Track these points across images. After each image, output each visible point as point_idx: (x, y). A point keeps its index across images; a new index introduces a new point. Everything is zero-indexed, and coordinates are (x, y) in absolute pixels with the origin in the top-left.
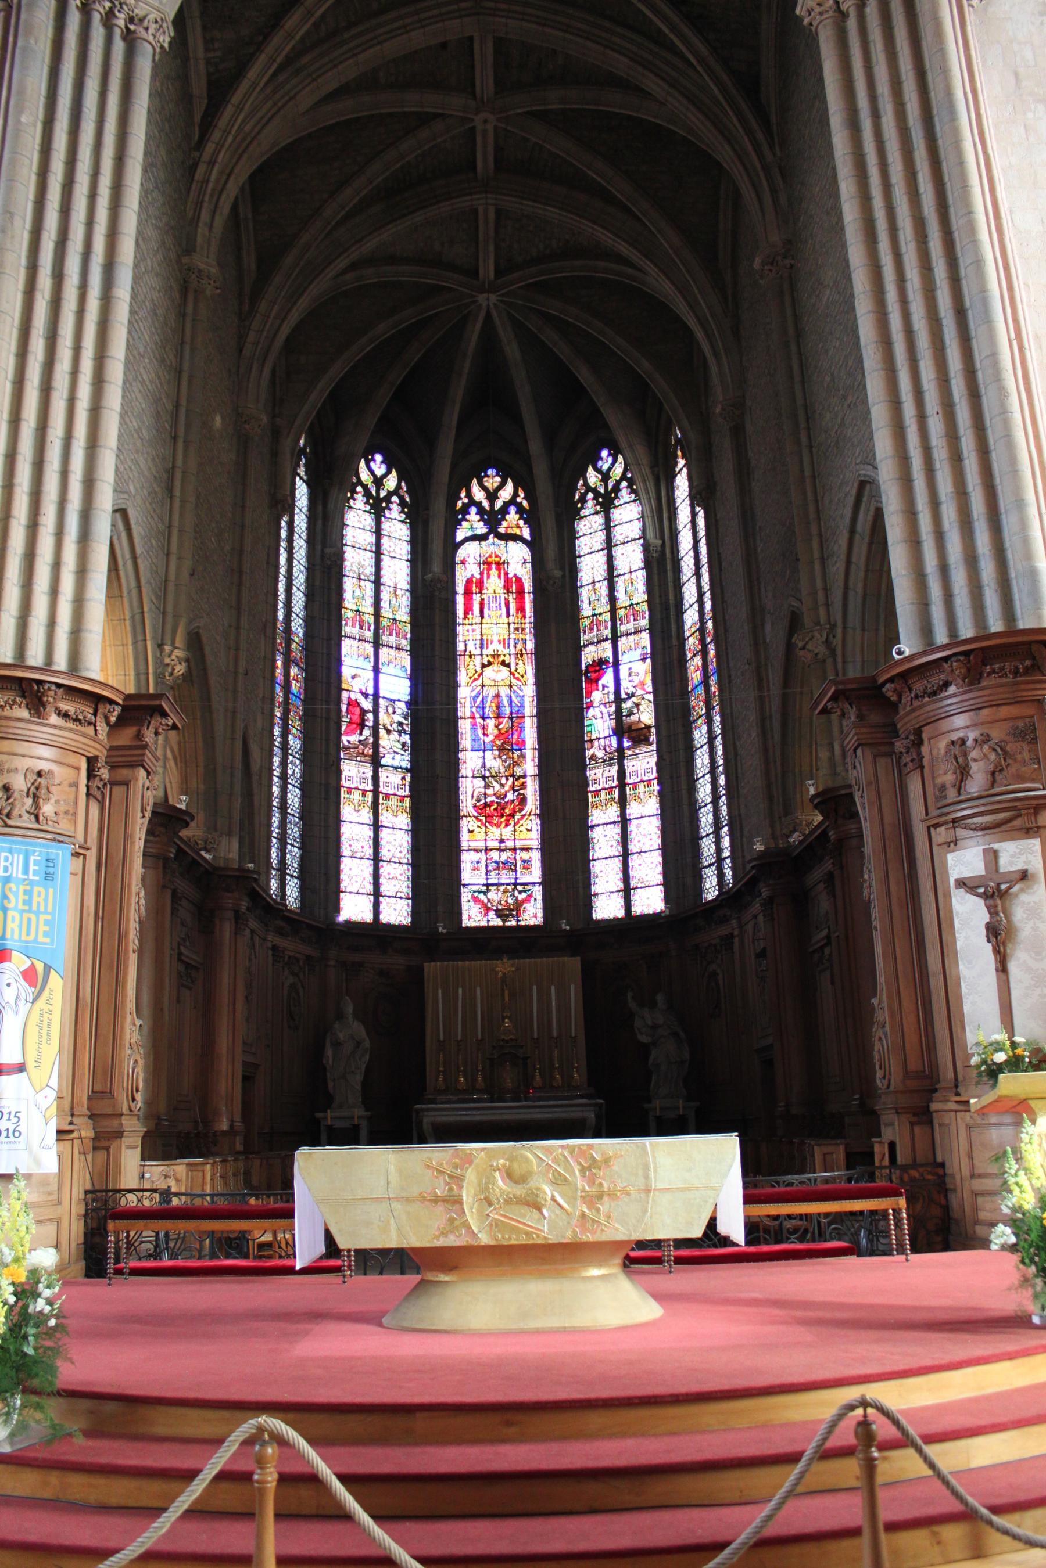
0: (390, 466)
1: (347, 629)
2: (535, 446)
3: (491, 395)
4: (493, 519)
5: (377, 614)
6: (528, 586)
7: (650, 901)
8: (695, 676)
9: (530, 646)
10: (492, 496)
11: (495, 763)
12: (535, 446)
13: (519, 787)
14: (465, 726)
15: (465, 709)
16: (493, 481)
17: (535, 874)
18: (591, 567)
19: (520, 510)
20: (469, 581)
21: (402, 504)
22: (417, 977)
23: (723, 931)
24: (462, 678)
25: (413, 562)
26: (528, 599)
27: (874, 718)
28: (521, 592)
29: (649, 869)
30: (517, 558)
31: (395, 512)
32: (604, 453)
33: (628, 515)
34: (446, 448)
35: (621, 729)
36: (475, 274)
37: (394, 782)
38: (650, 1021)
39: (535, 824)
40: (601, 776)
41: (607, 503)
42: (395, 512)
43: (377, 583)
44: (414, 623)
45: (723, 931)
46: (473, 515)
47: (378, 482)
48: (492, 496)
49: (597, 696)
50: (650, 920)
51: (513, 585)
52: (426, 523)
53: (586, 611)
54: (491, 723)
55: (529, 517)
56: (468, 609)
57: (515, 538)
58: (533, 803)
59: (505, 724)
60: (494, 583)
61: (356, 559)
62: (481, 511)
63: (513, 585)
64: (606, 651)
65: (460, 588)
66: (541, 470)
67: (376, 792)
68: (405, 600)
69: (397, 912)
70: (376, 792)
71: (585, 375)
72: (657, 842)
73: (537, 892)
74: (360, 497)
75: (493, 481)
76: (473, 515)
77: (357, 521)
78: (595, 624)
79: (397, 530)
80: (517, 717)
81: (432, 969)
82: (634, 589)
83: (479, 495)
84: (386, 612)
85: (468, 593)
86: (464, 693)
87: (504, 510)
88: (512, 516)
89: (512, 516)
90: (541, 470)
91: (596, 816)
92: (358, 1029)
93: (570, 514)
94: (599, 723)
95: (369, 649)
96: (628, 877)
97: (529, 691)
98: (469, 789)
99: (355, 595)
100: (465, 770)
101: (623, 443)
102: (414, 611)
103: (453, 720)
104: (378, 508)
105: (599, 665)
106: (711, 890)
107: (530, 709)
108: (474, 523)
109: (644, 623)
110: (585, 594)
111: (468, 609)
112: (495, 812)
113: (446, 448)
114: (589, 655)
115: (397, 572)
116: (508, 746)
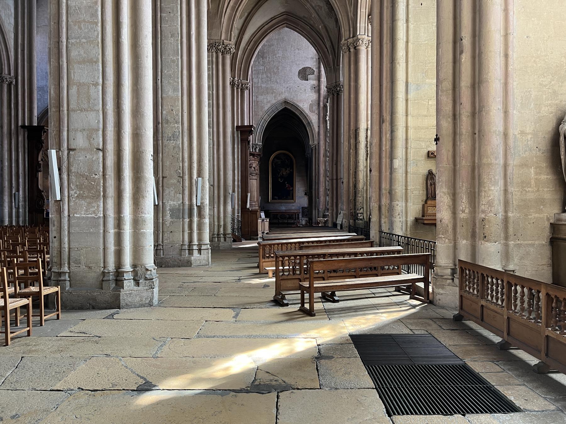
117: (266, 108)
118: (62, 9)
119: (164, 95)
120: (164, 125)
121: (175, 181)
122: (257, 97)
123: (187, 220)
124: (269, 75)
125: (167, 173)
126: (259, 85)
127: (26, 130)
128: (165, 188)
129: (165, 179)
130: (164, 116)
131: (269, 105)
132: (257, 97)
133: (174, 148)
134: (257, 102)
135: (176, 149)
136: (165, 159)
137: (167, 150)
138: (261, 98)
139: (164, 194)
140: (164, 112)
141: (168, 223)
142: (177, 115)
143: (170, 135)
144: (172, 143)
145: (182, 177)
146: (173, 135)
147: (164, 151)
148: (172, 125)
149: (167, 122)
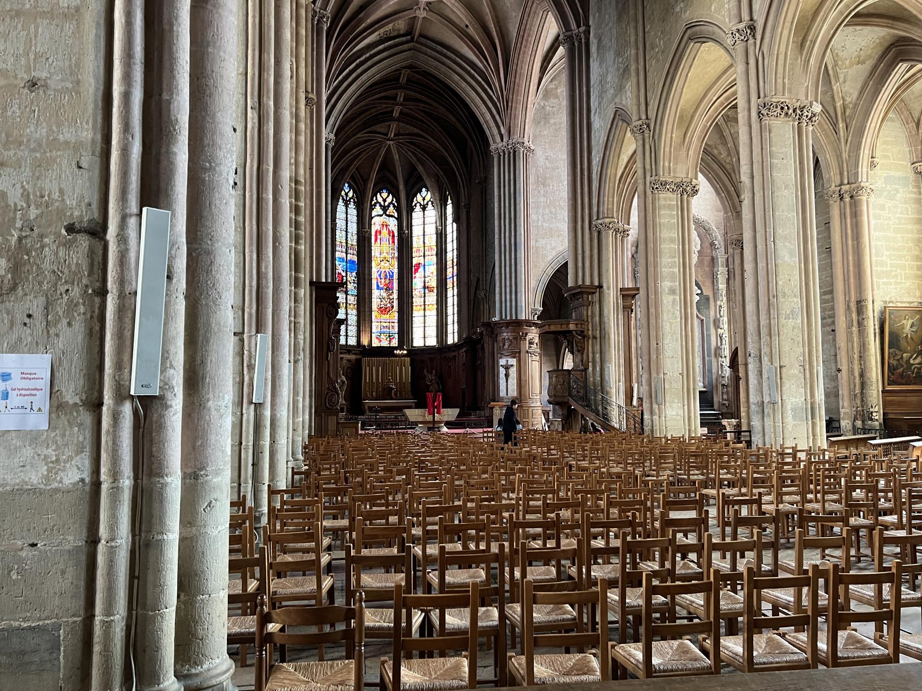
0: (350, 187)
1: (337, 248)
2: (401, 187)
3: (387, 167)
4: (385, 209)
5: (347, 243)
6: (396, 234)
7: (432, 342)
8: (449, 274)
9: (396, 255)
10: (385, 201)
11: (385, 295)
12: (401, 187)
14: (374, 282)
15: (375, 275)
16: (385, 195)
17: (396, 330)
18: (417, 231)
19: (394, 206)
20: (376, 232)
21: (354, 202)
22: (358, 362)
23: (453, 354)
24: (373, 264)
25: (358, 223)
26: (396, 238)
27: (489, 329)
28: (393, 236)
29: (432, 332)
30: (393, 224)
31: (352, 205)
32: (424, 189)
33: (432, 214)
34: (371, 185)
35: (425, 287)
36: (387, 135)
37: (352, 300)
38: (430, 377)
39: (396, 315)
40: (417, 301)
41: (424, 208)
42: (352, 205)
43: (347, 231)
44: (358, 245)
45: (453, 354)
46: (378, 207)
47: (347, 194)
48: (385, 201)
49: (417, 275)
50: (431, 348)
51: (391, 233)
52: (362, 210)
53: (415, 245)
54: (383, 281)
55: (398, 209)
56: (376, 240)
57: (392, 216)
58: (396, 308)
59: (387, 281)
61: (340, 223)
62: (381, 205)
63: (391, 233)
64: (421, 260)
65: (373, 233)
67: (346, 303)
68: (355, 237)
69: (352, 341)
70: (346, 303)
71: (420, 168)
72: (435, 324)
73: (396, 336)
74: (341, 200)
75: (385, 195)
76: (378, 207)
77: (341, 207)
78: (418, 250)
79: (353, 211)
81: (365, 360)
82: (432, 241)
83: (380, 200)
84: (349, 242)
85: (376, 236)
86: (374, 270)
87: (389, 206)
88: (391, 207)
89: (391, 207)
91: (415, 313)
92: (344, 378)
93: (411, 209)
94: (417, 283)
95: (344, 255)
96: (424, 334)
97: (396, 271)
99: (340, 236)
100: (374, 296)
101: (428, 185)
102: (358, 241)
104: (347, 206)
105: (418, 265)
106: (450, 341)
107: (396, 276)
108: (378, 210)
109: (435, 253)
110: (414, 239)
111: (376, 240)
112: (383, 310)
113: (371, 185)
115: (353, 228)
116: (388, 288)
117: (550, 258)
118: (172, 88)
119: (779, 262)
120: (781, 299)
121: (796, 372)
122: (536, 241)
123: (810, 423)
124: (553, 210)
125: (785, 361)
126: (540, 224)
127: (314, 288)
128: (784, 380)
129: (784, 370)
130: (779, 288)
131: (554, 253)
132: (536, 241)
133: (794, 328)
134: (537, 248)
135: (796, 330)
136: (783, 343)
137: (785, 331)
138: (542, 242)
139: (784, 389)
140: (780, 283)
141: (789, 427)
142: (796, 286)
143: (788, 312)
144: (791, 322)
145: (803, 366)
146: (792, 312)
147: (781, 333)
148: (790, 299)
149: (784, 295)
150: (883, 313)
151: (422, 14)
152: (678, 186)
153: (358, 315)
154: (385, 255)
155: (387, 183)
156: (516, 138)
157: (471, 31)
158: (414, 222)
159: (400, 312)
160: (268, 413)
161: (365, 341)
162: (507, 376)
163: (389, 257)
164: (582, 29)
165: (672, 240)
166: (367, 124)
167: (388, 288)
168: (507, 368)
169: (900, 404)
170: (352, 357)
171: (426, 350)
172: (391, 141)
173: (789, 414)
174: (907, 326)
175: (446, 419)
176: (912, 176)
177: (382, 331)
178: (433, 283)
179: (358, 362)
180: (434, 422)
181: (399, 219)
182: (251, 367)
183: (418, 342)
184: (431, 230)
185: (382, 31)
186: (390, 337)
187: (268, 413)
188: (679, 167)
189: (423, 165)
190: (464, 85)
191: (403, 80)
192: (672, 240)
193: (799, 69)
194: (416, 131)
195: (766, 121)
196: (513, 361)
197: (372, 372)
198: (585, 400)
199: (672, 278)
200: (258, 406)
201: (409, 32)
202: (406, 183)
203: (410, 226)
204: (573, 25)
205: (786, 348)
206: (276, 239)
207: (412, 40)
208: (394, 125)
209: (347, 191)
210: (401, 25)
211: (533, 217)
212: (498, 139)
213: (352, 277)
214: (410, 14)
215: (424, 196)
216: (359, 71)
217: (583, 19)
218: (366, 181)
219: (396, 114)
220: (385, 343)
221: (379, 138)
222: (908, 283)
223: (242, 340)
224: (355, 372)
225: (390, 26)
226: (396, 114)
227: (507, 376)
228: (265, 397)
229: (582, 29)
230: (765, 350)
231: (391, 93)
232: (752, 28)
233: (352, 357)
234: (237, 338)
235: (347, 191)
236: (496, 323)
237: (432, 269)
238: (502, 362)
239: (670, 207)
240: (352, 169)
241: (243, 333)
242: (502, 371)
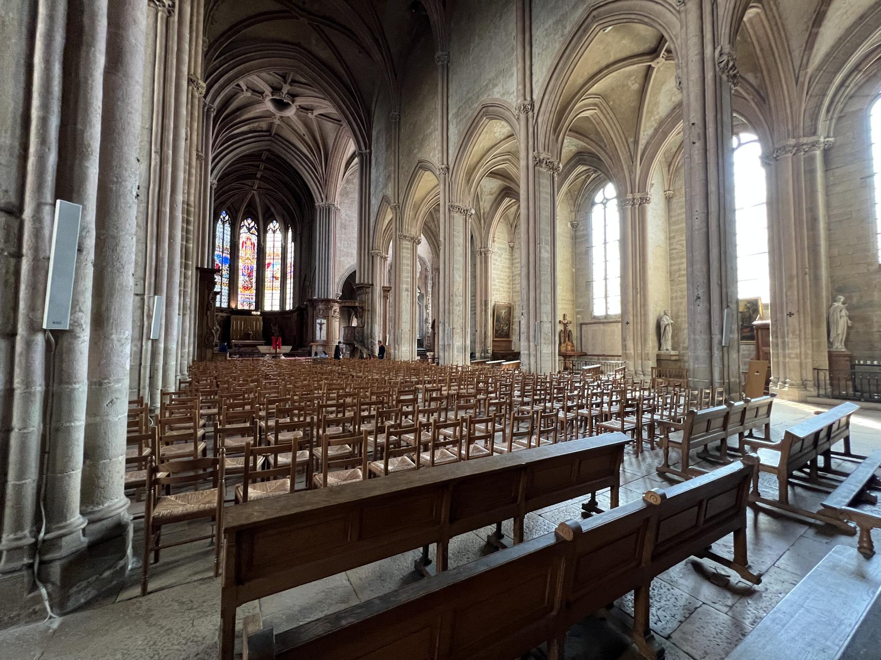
2: (260, 218)
4: (249, 230)
7: (277, 308)
12: (260, 218)
13: (251, 284)
22: (228, 318)
30: (254, 239)
31: (227, 225)
33: (279, 236)
34: (241, 214)
38: (275, 329)
40: (268, 284)
41: (274, 232)
55: (258, 230)
60: (249, 243)
61: (219, 234)
65: (241, 243)
66: (261, 223)
69: (225, 305)
71: (273, 209)
75: (249, 221)
79: (228, 227)
80: (252, 271)
81: (233, 317)
83: (246, 224)
90: (261, 223)
91: (266, 291)
93: (265, 232)
94: (268, 274)
96: (272, 303)
97: (255, 266)
98: (240, 285)
99: (218, 242)
102: (231, 246)
103: (238, 269)
105: (269, 264)
108: (244, 230)
112: (246, 288)
113: (241, 214)
114: (267, 262)
115: (228, 238)
116: (250, 276)
125: (455, 326)
131: (349, 265)
138: (342, 259)
144: (458, 308)
150: (494, 307)
151: (277, 122)
152: (412, 238)
153: (229, 290)
154: (248, 256)
155: (251, 213)
156: (330, 201)
157: (306, 138)
158: (268, 239)
159: (257, 289)
160: (162, 346)
161: (233, 306)
162: (321, 329)
163: (251, 257)
164: (368, 151)
165: (408, 265)
166: (239, 178)
167: (250, 276)
168: (321, 324)
169: (499, 346)
170: (225, 315)
171: (272, 313)
172: (254, 192)
173: (456, 350)
174: (503, 312)
175: (284, 351)
176: (508, 248)
177: (245, 300)
178: (279, 275)
179: (228, 318)
180: (276, 353)
181: (258, 236)
182: (150, 317)
183: (267, 308)
184: (279, 245)
185: (251, 126)
186: (250, 304)
187: (162, 346)
188: (413, 229)
189: (274, 207)
190: (301, 167)
191: (264, 157)
192: (408, 265)
193: (466, 192)
194: (271, 187)
195: (452, 214)
196: (324, 321)
197: (237, 324)
198: (362, 343)
199: (407, 283)
200: (155, 342)
201: (269, 130)
202: (264, 216)
203: (265, 241)
204: (363, 148)
205: (455, 320)
206: (171, 237)
207: (270, 135)
208: (257, 182)
209: (224, 215)
210: (264, 125)
211: (338, 244)
212: (320, 200)
213: (225, 268)
214: (270, 120)
215: (274, 225)
216: (235, 146)
217: (368, 146)
218: (237, 212)
219: (258, 176)
220: (246, 308)
221: (247, 188)
222: (505, 294)
223: (143, 300)
224: (226, 324)
225: (257, 124)
226: (258, 176)
227: (321, 329)
228: (160, 336)
229: (368, 151)
230: (447, 320)
231: (257, 163)
232: (448, 169)
233: (225, 315)
234: (138, 298)
235: (224, 215)
236: (315, 300)
237: (278, 267)
238: (318, 321)
239: (407, 249)
240: (228, 203)
241: (144, 294)
242: (318, 326)
